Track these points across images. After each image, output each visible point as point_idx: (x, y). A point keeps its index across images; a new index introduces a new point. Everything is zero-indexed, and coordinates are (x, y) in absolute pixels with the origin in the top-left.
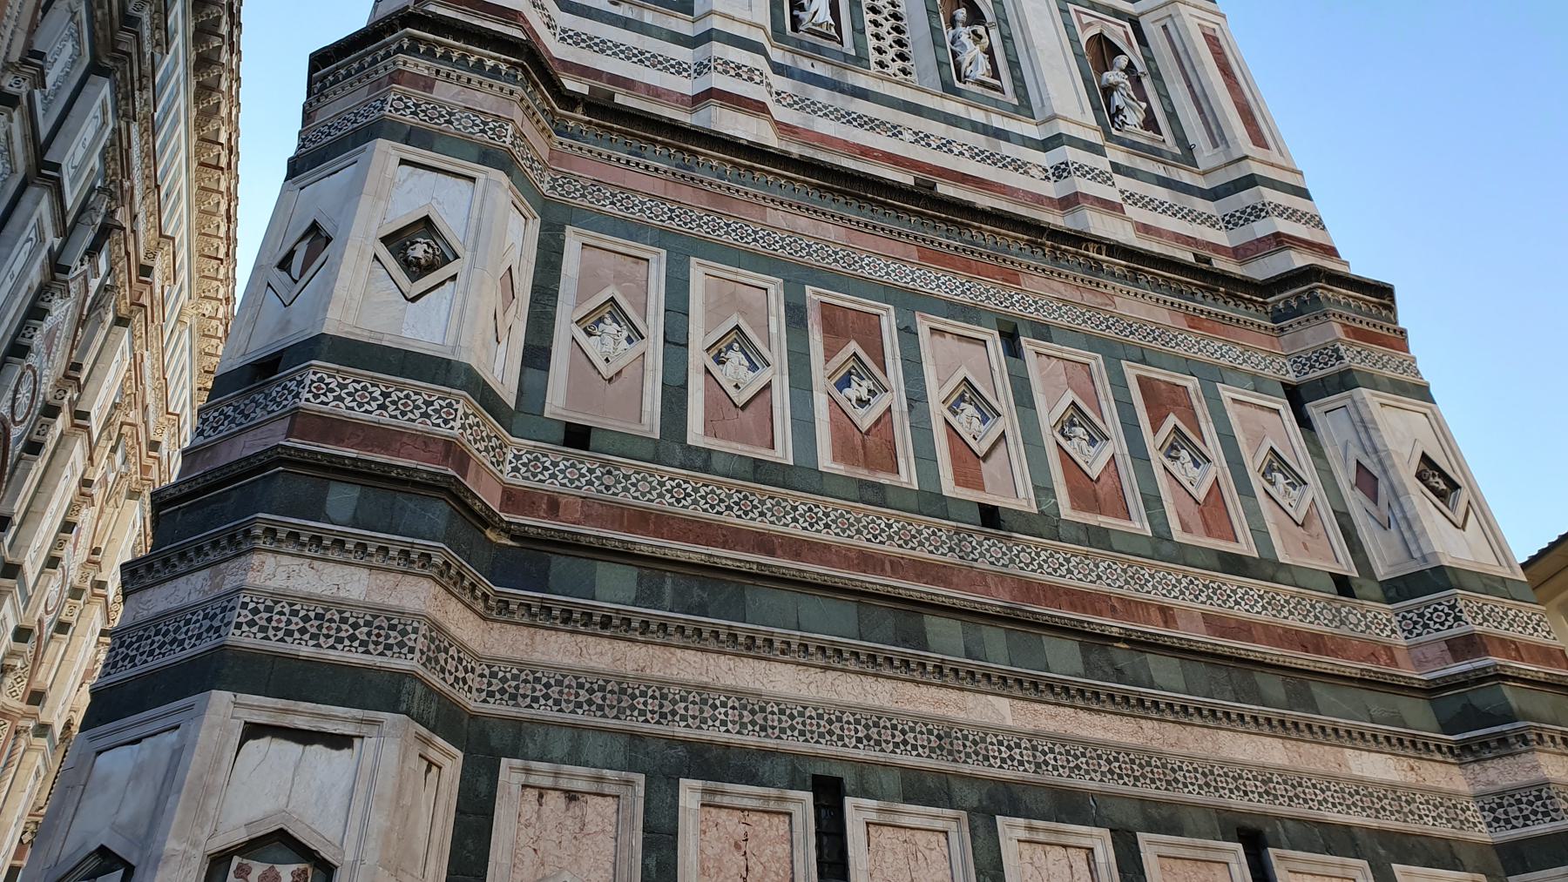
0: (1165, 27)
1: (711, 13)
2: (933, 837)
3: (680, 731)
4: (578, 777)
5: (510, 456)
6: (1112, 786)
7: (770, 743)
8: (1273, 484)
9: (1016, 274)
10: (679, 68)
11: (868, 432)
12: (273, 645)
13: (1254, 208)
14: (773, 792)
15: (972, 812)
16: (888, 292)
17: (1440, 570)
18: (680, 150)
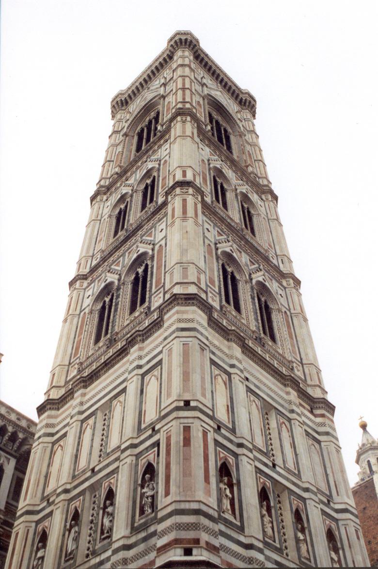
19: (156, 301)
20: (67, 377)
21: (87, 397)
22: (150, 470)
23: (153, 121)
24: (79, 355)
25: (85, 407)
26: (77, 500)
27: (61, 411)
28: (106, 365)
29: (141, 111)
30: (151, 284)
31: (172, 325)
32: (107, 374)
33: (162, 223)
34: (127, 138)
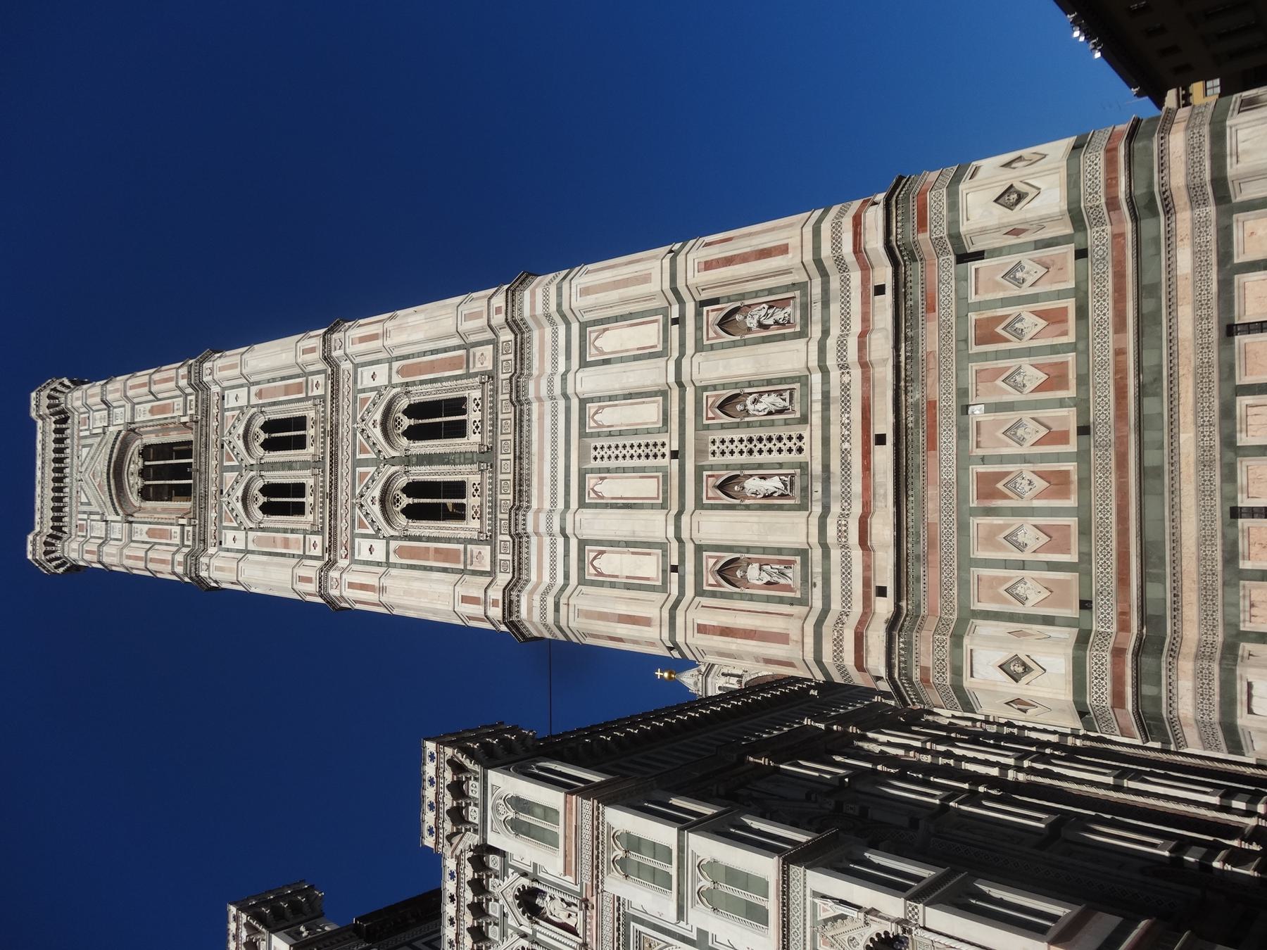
0: (703, 290)
1: (808, 543)
2: (1250, 472)
3: (1219, 567)
4: (1243, 604)
5: (1103, 630)
6: (1215, 392)
7: (1219, 535)
8: (1024, 280)
9: (929, 403)
10: (846, 559)
11: (1049, 482)
12: (1217, 708)
13: (836, 260)
14: (1240, 534)
15: (1237, 455)
16: (962, 467)
17: (1070, 211)
18: (907, 561)
19: (482, 364)
20: (482, 573)
21: (547, 506)
22: (726, 323)
23: (147, 463)
24: (461, 547)
25: (561, 505)
26: (704, 484)
27: (534, 577)
28: (520, 458)
29: (109, 485)
30: (448, 379)
31: (546, 296)
32: (535, 459)
33: (362, 377)
34: (135, 515)
